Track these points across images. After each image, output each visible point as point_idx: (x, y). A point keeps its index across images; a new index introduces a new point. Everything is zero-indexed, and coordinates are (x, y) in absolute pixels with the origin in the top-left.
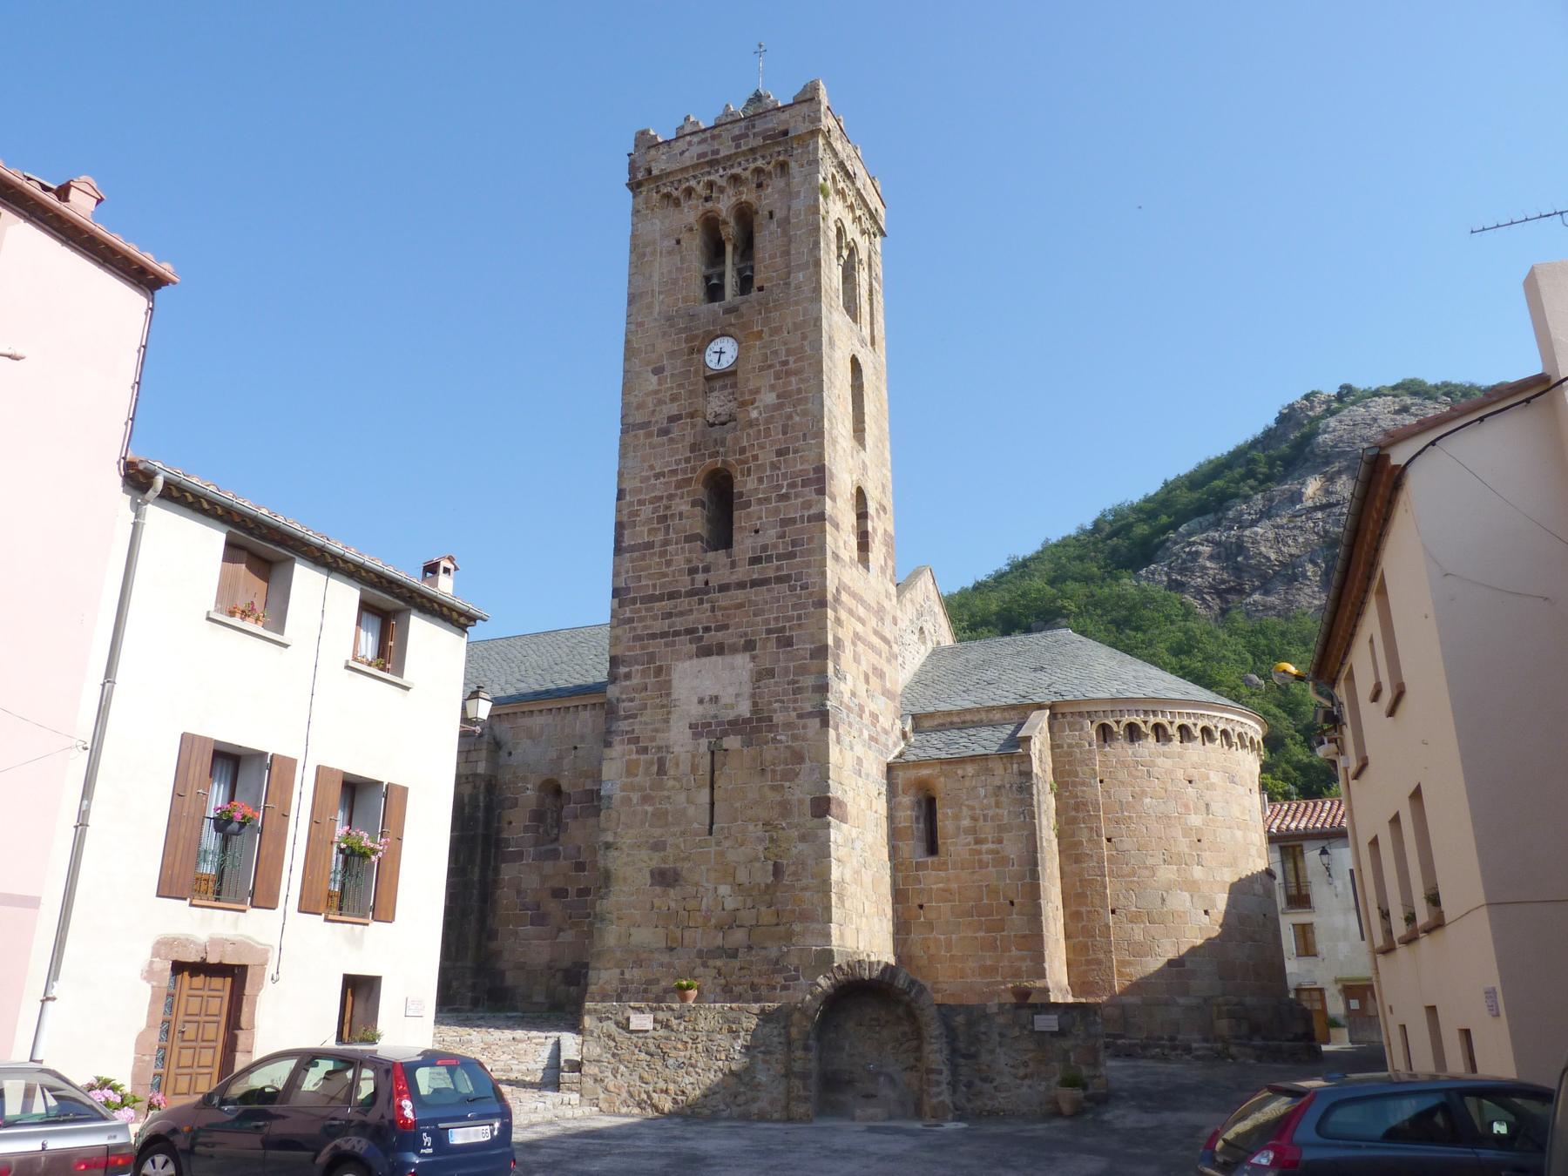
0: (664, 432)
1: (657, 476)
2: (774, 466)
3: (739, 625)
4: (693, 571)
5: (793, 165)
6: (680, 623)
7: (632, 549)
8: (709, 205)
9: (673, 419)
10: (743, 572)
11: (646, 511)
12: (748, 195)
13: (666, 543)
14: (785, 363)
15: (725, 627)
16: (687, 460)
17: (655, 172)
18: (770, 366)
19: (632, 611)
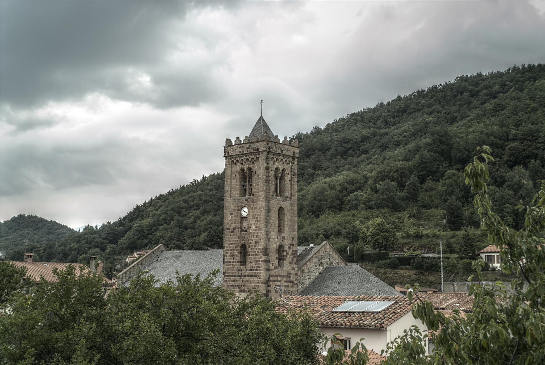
0: (233, 232)
1: (232, 244)
2: (255, 246)
3: (247, 286)
4: (239, 270)
5: (260, 159)
6: (237, 283)
7: (227, 262)
8: (242, 166)
9: (235, 229)
10: (248, 272)
11: (229, 253)
12: (251, 166)
13: (233, 262)
14: (257, 218)
15: (244, 286)
16: (237, 241)
17: (230, 154)
18: (254, 218)
19: (227, 279)
